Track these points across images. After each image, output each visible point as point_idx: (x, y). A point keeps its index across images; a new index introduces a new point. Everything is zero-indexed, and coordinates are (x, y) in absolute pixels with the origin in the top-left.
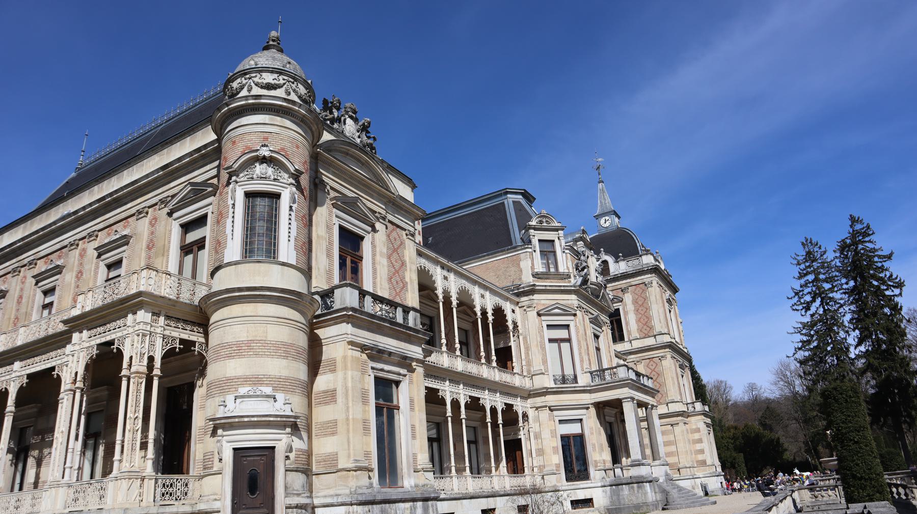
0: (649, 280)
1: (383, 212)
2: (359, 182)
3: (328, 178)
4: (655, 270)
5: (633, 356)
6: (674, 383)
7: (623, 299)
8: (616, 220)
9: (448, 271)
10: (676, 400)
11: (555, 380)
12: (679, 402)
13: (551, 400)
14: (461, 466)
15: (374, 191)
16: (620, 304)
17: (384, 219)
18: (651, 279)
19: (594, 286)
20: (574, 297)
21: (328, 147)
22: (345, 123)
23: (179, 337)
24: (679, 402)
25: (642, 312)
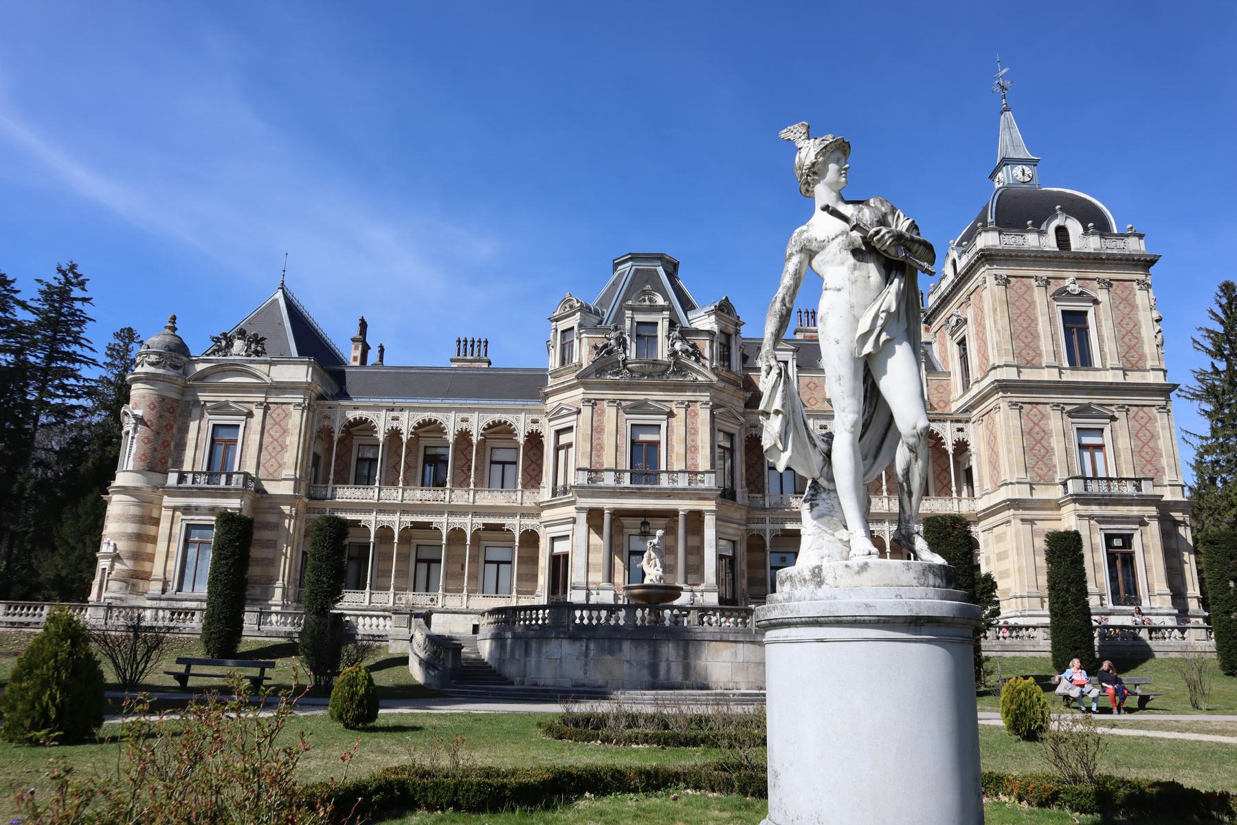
0: (981, 279)
1: (263, 400)
3: (203, 397)
4: (987, 257)
5: (975, 412)
6: (1009, 451)
7: (966, 321)
8: (1017, 170)
9: (401, 410)
10: (1008, 481)
11: (554, 493)
12: (1011, 483)
13: (547, 515)
16: (965, 327)
17: (261, 404)
18: (983, 275)
20: (581, 390)
21: (203, 376)
22: (232, 345)
24: (1011, 483)
25: (981, 335)
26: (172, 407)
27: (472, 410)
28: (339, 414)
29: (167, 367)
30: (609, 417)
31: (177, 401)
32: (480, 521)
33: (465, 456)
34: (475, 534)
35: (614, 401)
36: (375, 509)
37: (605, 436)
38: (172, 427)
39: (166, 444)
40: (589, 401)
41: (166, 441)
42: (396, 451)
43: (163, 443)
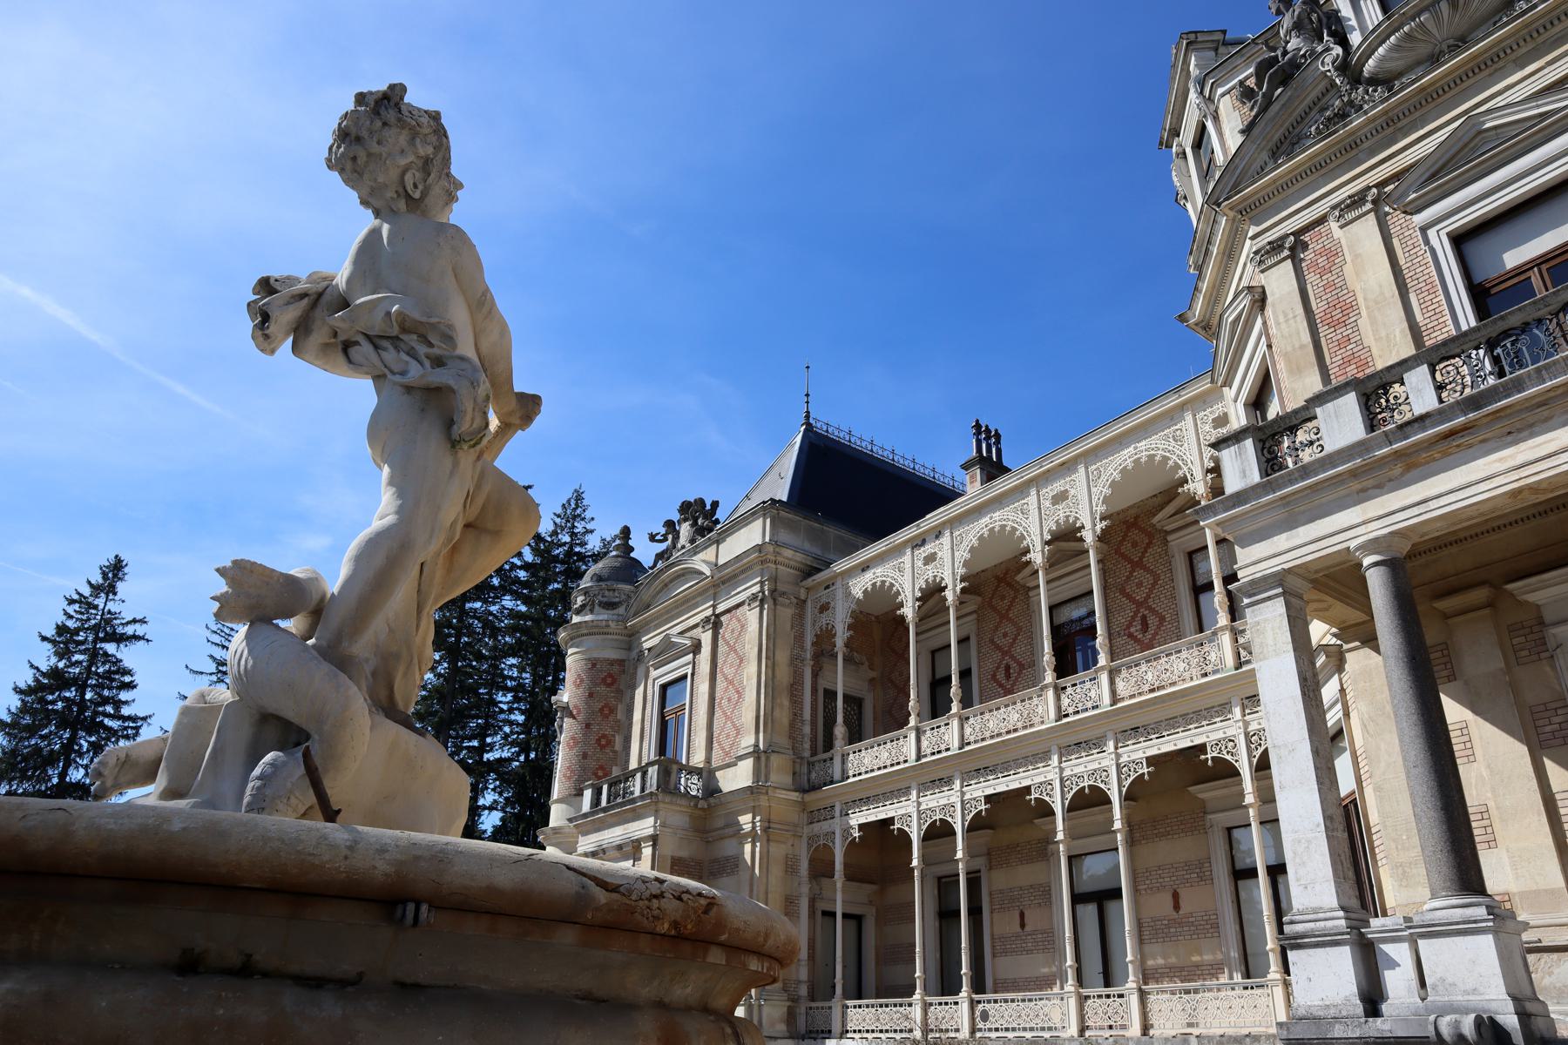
1: (709, 612)
2: (677, 607)
14: (1206, 957)
15: (694, 598)
17: (707, 620)
19: (1381, 50)
23: (1146, 755)
26: (610, 675)
27: (1067, 467)
28: (840, 594)
29: (597, 607)
30: (1356, 256)
31: (621, 662)
32: (1140, 752)
33: (1128, 596)
34: (1129, 797)
35: (1357, 200)
36: (914, 785)
37: (1364, 323)
38: (612, 711)
39: (603, 742)
40: (1276, 246)
41: (604, 736)
42: (992, 641)
43: (598, 741)
